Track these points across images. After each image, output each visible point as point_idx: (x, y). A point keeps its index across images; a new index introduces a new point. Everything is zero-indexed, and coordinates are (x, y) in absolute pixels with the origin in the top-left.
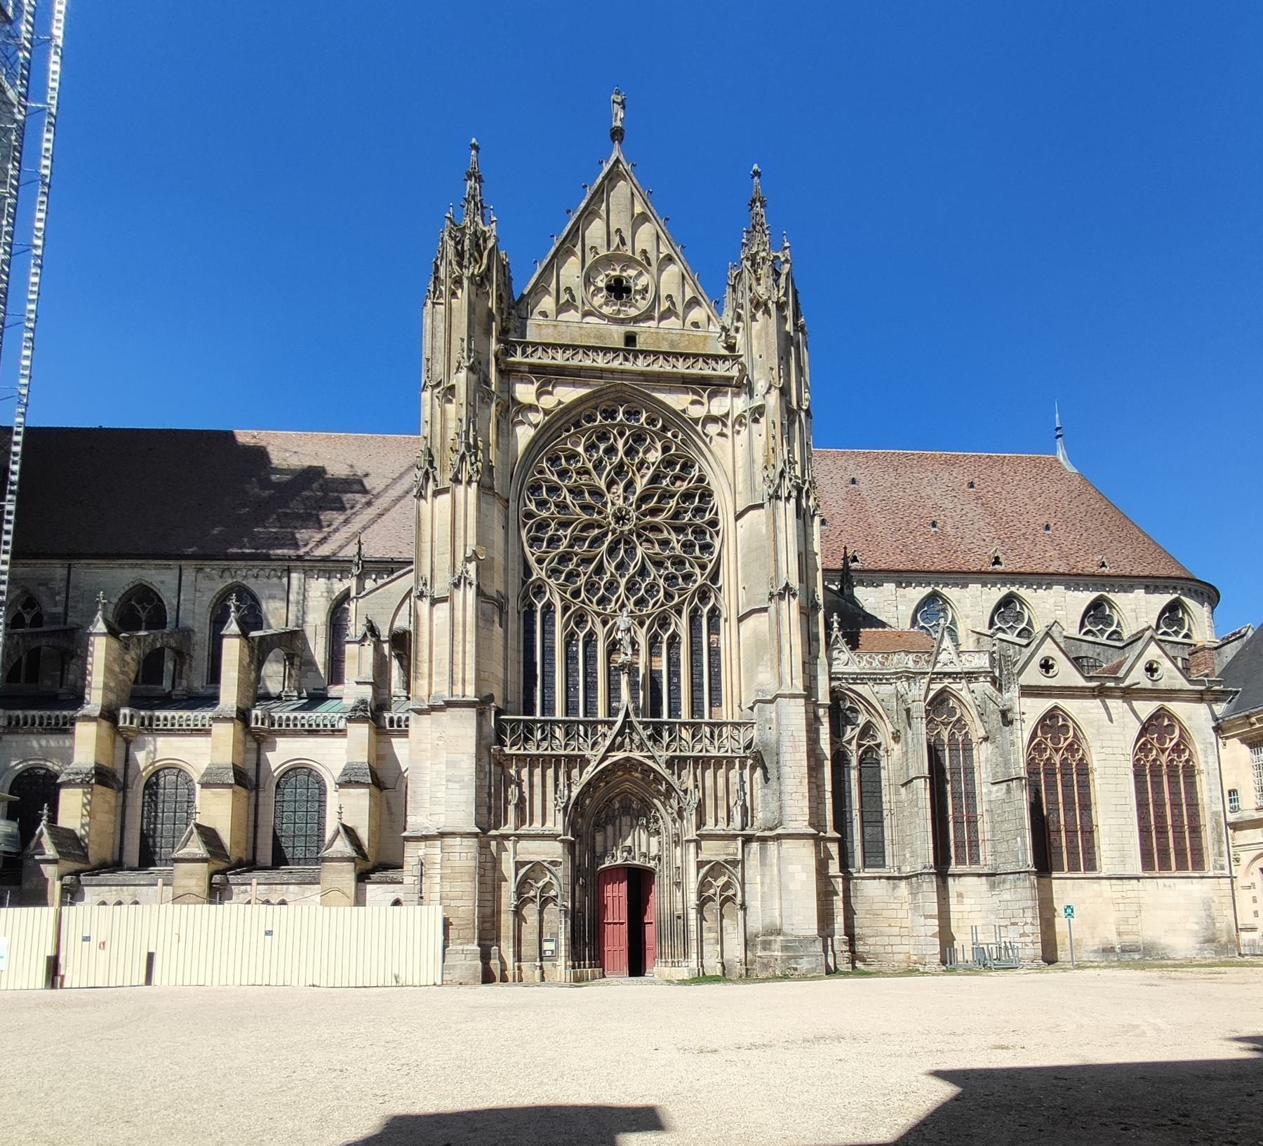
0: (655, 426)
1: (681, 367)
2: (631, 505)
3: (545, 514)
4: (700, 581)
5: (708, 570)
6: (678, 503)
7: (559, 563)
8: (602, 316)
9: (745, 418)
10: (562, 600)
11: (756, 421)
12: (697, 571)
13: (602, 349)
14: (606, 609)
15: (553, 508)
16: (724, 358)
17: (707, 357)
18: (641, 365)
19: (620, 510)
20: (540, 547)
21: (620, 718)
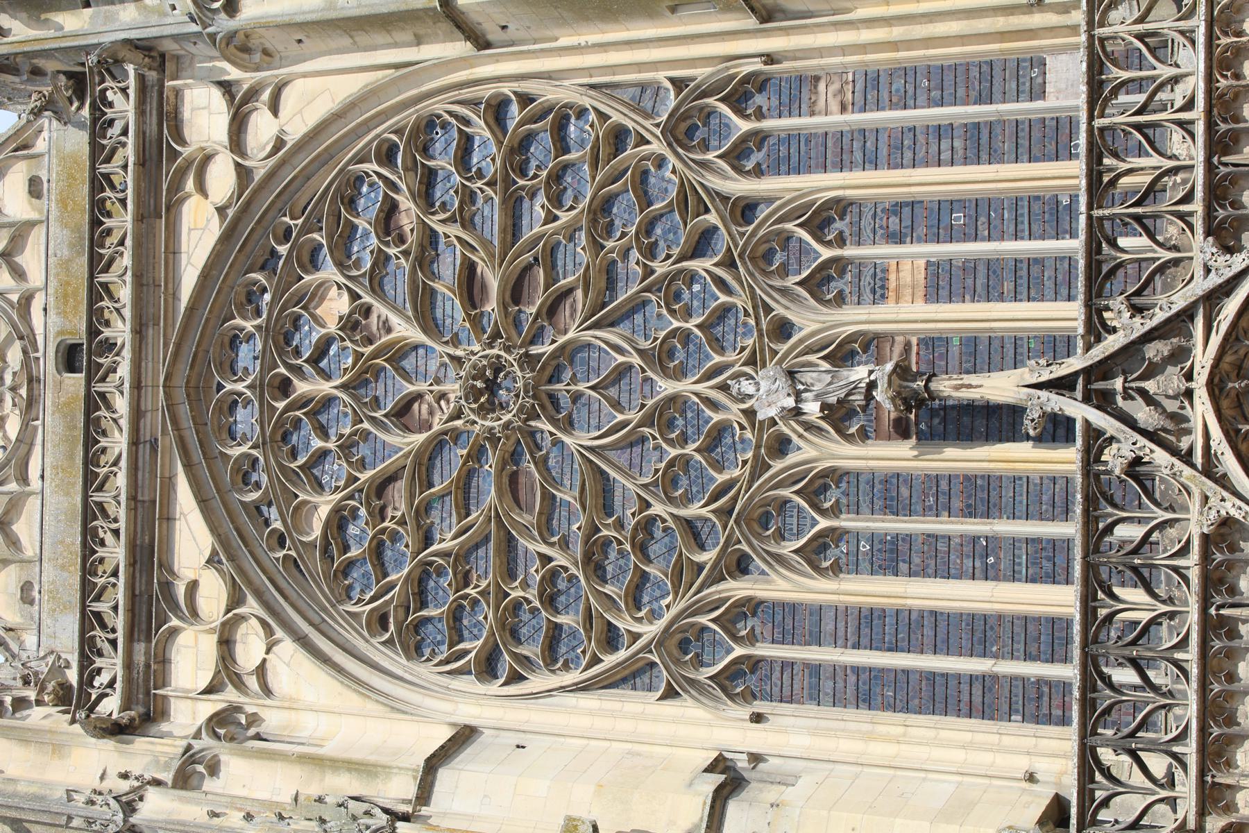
1: (123, 221)
2: (458, 360)
3: (487, 615)
4: (657, 146)
6: (452, 219)
13: (89, 442)
17: (99, 153)
18: (120, 331)
19: (472, 394)
20: (573, 633)
21: (1078, 410)
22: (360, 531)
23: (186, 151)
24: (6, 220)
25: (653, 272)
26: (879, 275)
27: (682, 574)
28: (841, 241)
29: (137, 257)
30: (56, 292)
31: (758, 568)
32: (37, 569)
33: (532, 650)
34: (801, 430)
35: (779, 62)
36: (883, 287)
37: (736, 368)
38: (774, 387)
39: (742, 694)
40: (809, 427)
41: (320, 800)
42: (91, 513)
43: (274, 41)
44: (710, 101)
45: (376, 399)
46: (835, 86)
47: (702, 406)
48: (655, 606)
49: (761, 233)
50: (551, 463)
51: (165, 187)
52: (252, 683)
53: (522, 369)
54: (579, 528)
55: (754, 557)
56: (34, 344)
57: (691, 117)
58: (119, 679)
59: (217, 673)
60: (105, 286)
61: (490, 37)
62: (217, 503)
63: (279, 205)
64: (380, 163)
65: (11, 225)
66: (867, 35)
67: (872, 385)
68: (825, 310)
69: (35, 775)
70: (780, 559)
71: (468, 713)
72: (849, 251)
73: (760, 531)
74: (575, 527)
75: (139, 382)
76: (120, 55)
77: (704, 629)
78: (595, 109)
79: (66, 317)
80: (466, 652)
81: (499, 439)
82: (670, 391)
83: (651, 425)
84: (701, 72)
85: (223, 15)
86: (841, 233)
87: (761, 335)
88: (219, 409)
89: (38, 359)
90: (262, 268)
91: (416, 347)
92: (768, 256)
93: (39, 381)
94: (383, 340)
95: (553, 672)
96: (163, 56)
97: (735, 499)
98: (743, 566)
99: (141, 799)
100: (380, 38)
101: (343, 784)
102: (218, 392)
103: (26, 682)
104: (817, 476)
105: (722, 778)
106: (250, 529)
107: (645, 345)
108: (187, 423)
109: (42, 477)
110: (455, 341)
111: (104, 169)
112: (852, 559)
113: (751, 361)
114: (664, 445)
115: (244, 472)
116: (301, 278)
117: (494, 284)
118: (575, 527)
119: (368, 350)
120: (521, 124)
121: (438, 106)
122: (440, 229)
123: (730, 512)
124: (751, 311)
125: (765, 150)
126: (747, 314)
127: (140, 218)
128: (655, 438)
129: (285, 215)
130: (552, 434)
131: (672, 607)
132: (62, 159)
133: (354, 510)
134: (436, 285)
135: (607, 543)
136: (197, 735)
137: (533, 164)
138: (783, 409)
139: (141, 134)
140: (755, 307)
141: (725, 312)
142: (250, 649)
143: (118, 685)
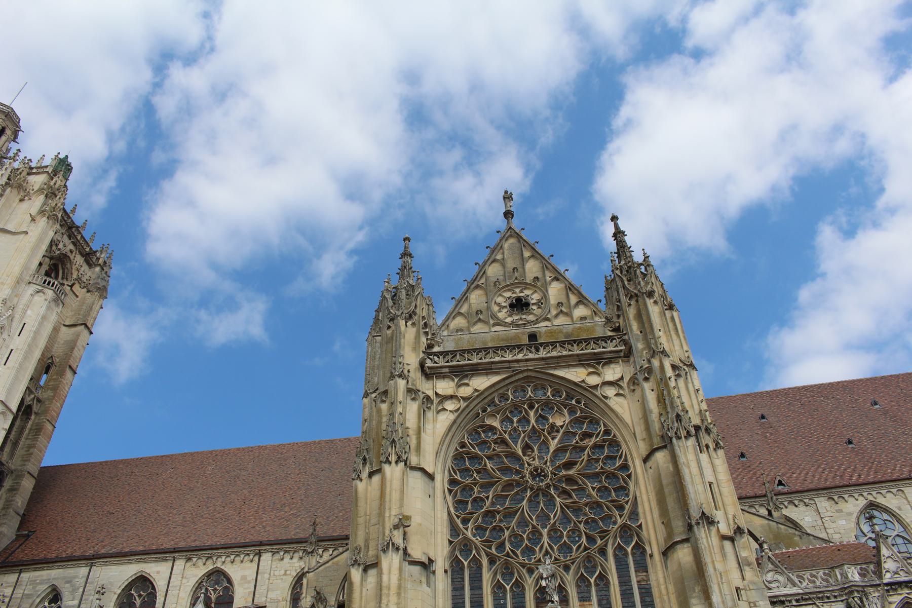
0: (561, 397)
1: (576, 351)
2: (546, 462)
3: (468, 481)
5: (625, 512)
6: (589, 456)
7: (483, 521)
8: (506, 325)
9: (637, 379)
10: (488, 554)
11: (646, 379)
12: (616, 513)
13: (508, 347)
14: (531, 559)
15: (475, 475)
16: (611, 338)
17: (598, 339)
18: (543, 353)
19: (536, 469)
20: (466, 509)
22: (491, 437)
23: (600, 368)
24: (572, 310)
25: (580, 524)
26: (587, 599)
27: (488, 543)
28: (597, 585)
29: (566, 356)
30: (552, 329)
31: (492, 567)
32: (467, 333)
33: (459, 497)
34: (536, 578)
35: (650, 559)
36: (584, 601)
37: (553, 555)
38: (549, 570)
39: (453, 566)
40: (537, 581)
41: (408, 436)
42: (486, 350)
43: (638, 392)
44: (636, 538)
45: (531, 437)
46: (645, 579)
47: (540, 545)
48: (477, 535)
49: (597, 559)
50: (518, 496)
51: (588, 362)
52: (440, 408)
53: (545, 484)
54: (498, 508)
55: (495, 567)
56: (536, 324)
57: (630, 531)
58: (437, 365)
59: (442, 396)
60: (556, 346)
61: (647, 463)
62: (493, 389)
63: (587, 399)
64: (604, 431)
65: (571, 312)
66: (663, 587)
67: (553, 602)
68: (574, 582)
69: (406, 343)
70: (495, 574)
71: (438, 478)
72: (593, 589)
73: (504, 567)
74: (498, 506)
75: (528, 361)
76: (627, 346)
77: (471, 551)
78: (629, 499)
79: (544, 334)
80: (456, 475)
81: (523, 479)
82: (543, 533)
83: (532, 528)
84: (644, 533)
85: (644, 377)
86: (599, 585)
87: (564, 562)
88: (522, 387)
89: (531, 326)
90: (567, 395)
91: (548, 448)
92: (589, 561)
93: (525, 327)
94: (549, 438)
95: (453, 504)
96: (629, 357)
97: (512, 558)
98: (492, 562)
99: (403, 379)
100: (643, 427)
101: (413, 442)
102: (527, 385)
103: (433, 334)
104: (522, 584)
105: (427, 564)
106: (486, 401)
107: (557, 524)
108: (517, 377)
109: (495, 331)
110: (551, 461)
111: (592, 342)
112: (498, 598)
113: (556, 559)
114: (527, 533)
115: (504, 397)
116: (566, 409)
117: (571, 472)
118: (498, 506)
119: (546, 433)
120: (622, 476)
121: (624, 447)
122: (586, 452)
123: (508, 557)
124: (572, 558)
125: (623, 557)
126: (571, 556)
127: (578, 355)
128: (529, 530)
129: (584, 401)
130: (526, 496)
131: (477, 540)
132: (593, 327)
133: (496, 434)
134: (568, 454)
135: (494, 517)
136: (423, 393)
137: (610, 481)
138: (542, 574)
139: (604, 353)
140: (573, 559)
141: (571, 549)
142: (450, 405)
143: (435, 365)
